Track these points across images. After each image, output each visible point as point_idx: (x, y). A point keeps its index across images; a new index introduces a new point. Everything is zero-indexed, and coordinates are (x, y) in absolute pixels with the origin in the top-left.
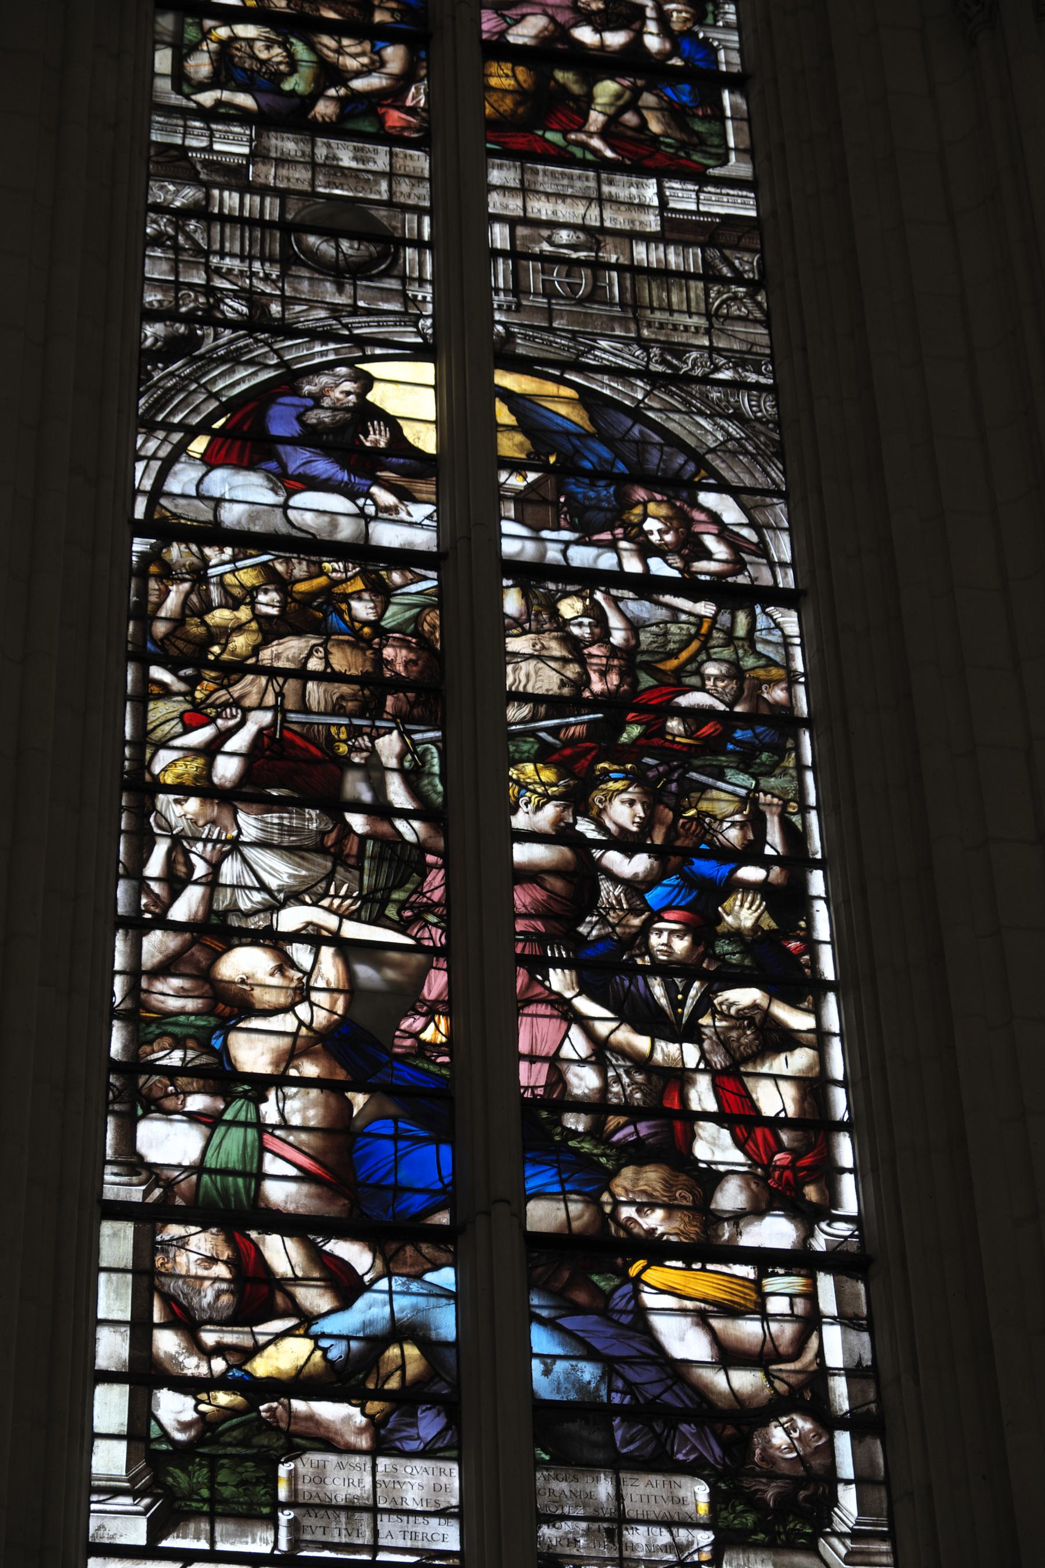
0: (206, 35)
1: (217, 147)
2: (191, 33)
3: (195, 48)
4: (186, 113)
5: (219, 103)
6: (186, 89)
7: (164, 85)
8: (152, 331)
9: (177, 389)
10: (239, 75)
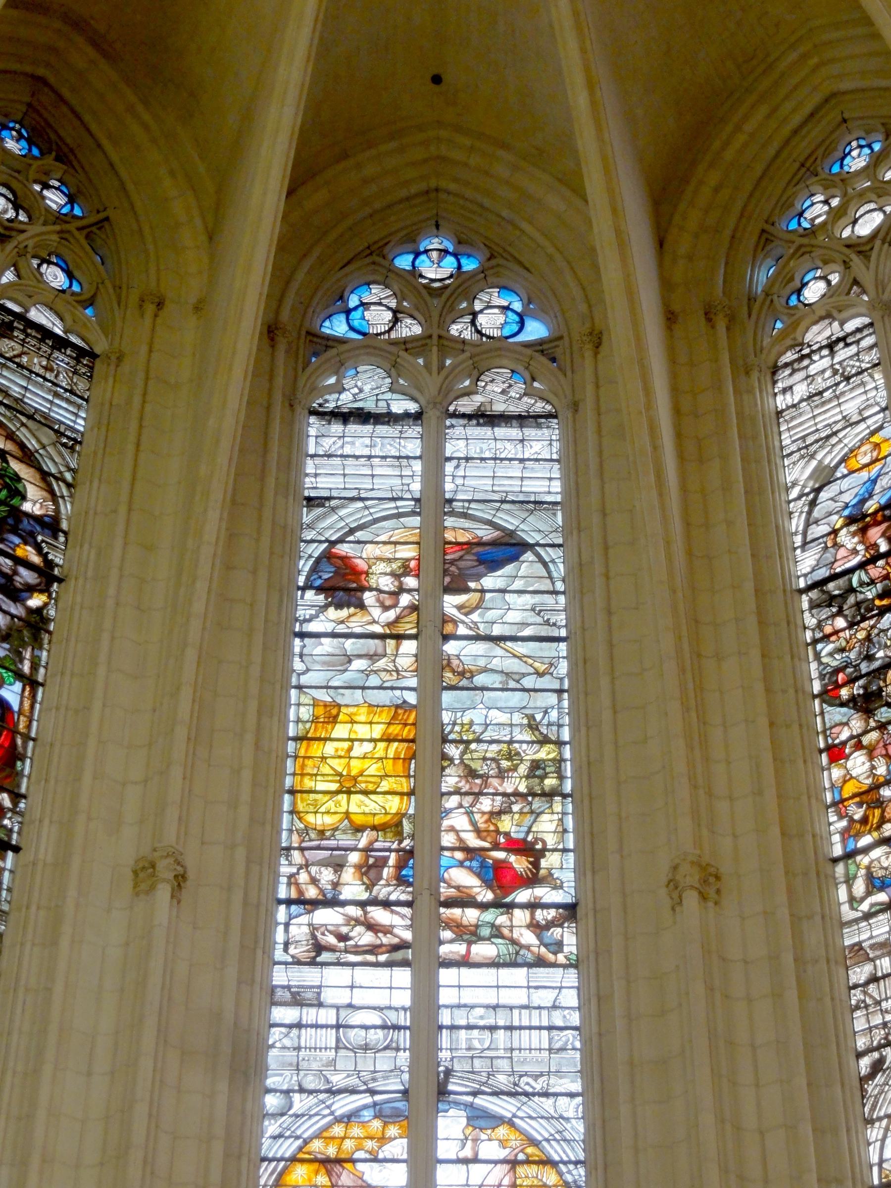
0: (858, 866)
1: (874, 934)
2: (852, 868)
3: (855, 877)
4: (856, 921)
5: (872, 905)
6: (855, 905)
7: (845, 908)
8: (865, 1063)
9: (880, 1093)
10: (877, 883)
